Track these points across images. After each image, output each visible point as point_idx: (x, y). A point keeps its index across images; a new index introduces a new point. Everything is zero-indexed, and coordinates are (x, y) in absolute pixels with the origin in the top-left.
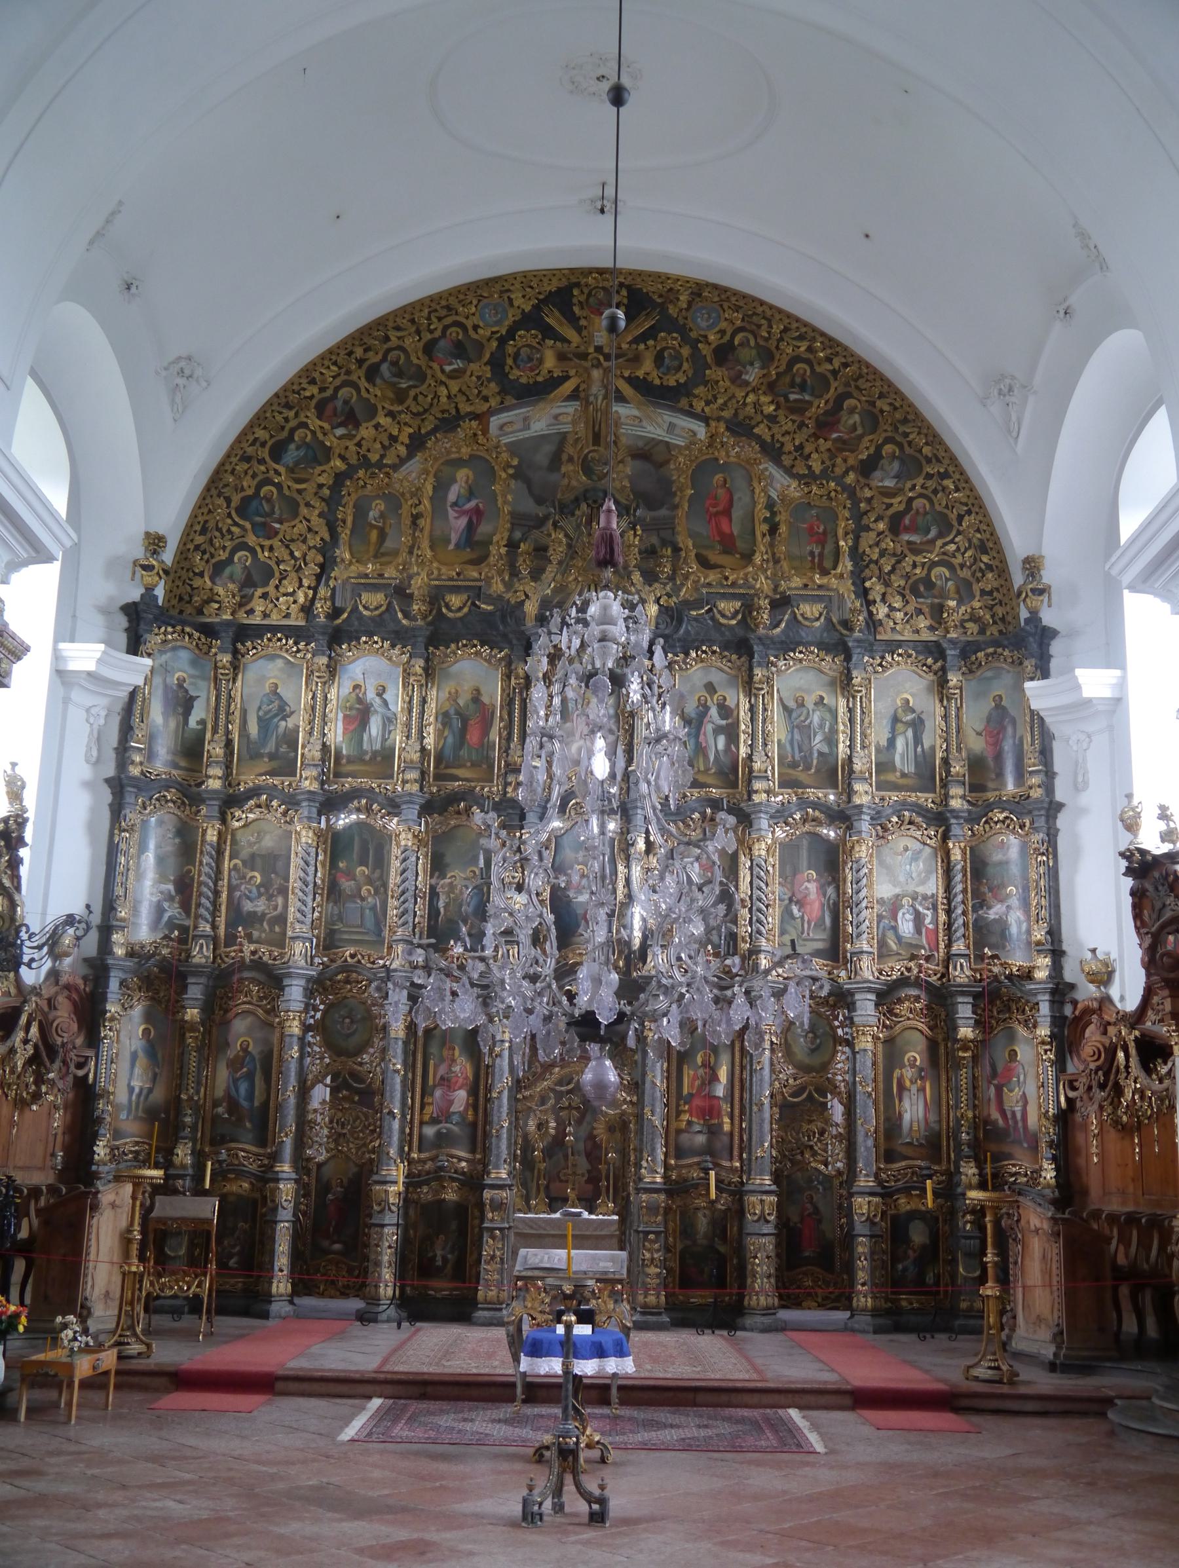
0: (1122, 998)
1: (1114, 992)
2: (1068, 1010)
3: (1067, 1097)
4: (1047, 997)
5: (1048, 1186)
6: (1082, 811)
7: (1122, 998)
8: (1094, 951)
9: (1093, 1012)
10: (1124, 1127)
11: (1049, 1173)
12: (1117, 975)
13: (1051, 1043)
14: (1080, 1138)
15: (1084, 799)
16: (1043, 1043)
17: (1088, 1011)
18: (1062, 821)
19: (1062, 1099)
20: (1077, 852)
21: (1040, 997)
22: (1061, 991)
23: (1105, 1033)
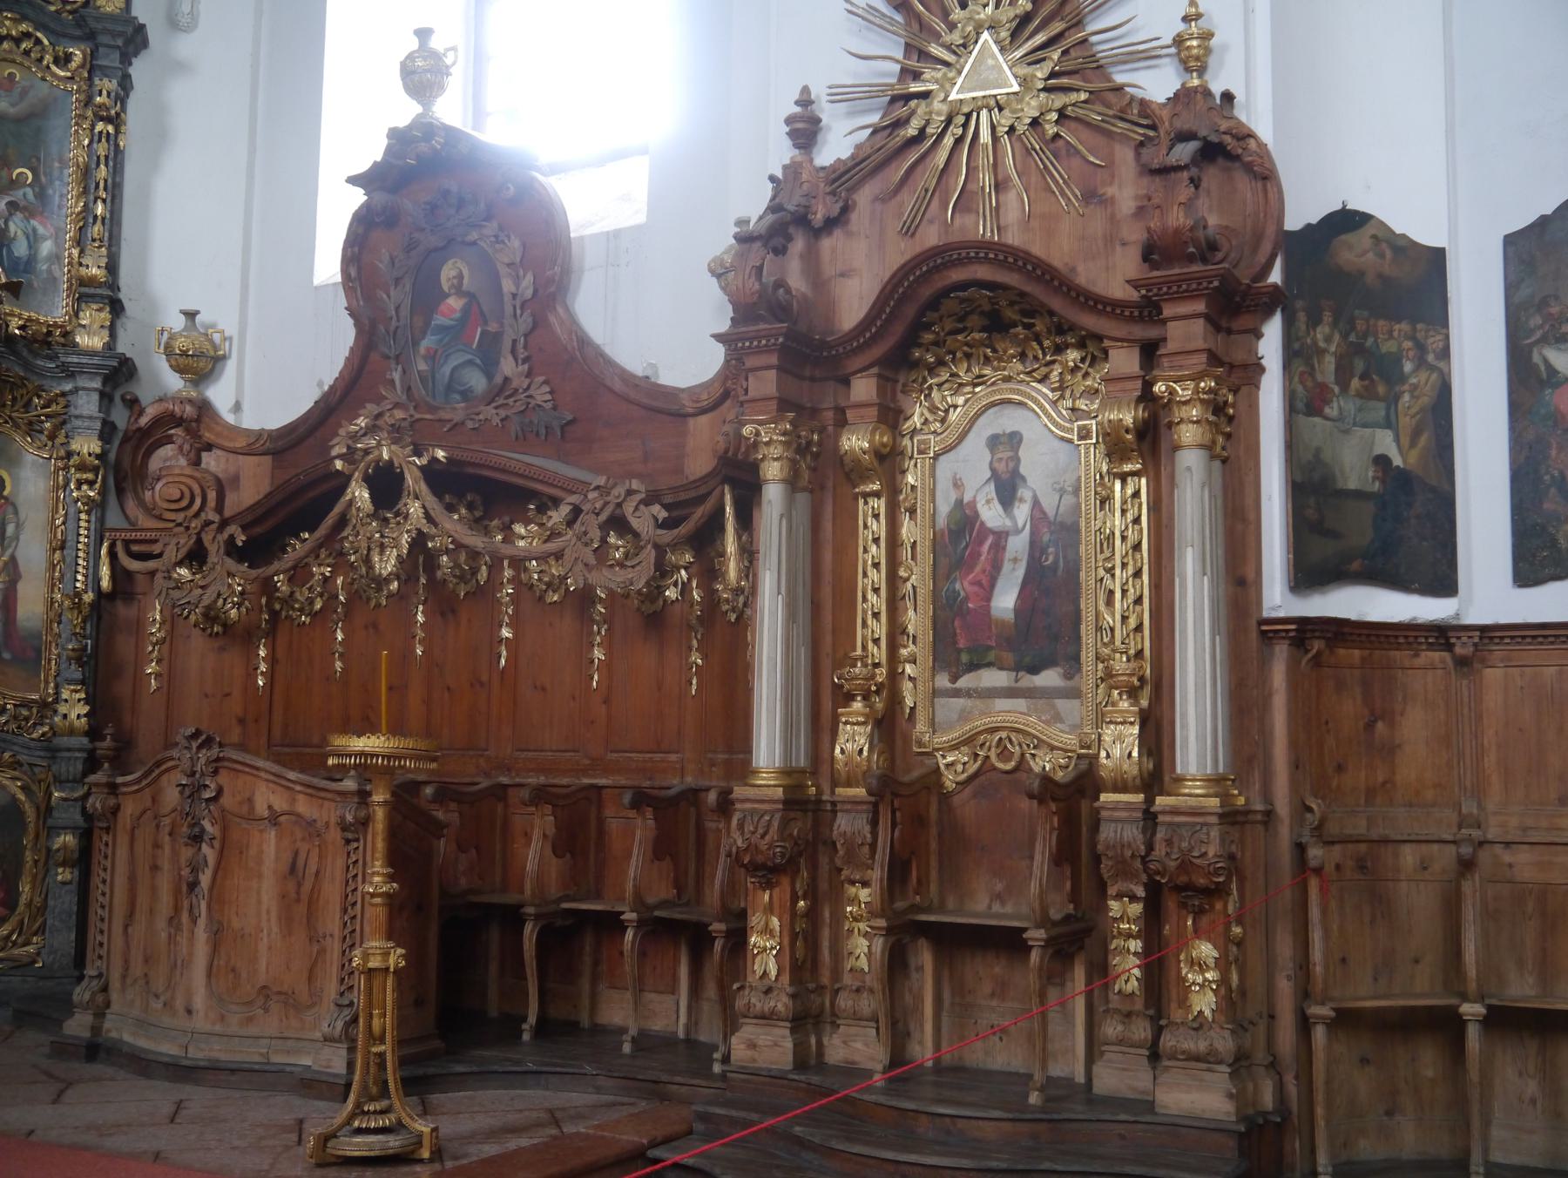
0: (237, 407)
1: (220, 395)
2: (120, 417)
3: (117, 571)
4: (97, 384)
5: (72, 732)
6: (180, 67)
7: (237, 407)
8: (191, 315)
9: (179, 421)
10: (227, 627)
11: (74, 709)
12: (231, 367)
13: (95, 470)
14: (124, 646)
15: (185, 46)
16: (81, 467)
17: (168, 420)
18: (140, 69)
19: (105, 571)
20: (161, 137)
21: (82, 382)
22: (119, 373)
23: (197, 462)
